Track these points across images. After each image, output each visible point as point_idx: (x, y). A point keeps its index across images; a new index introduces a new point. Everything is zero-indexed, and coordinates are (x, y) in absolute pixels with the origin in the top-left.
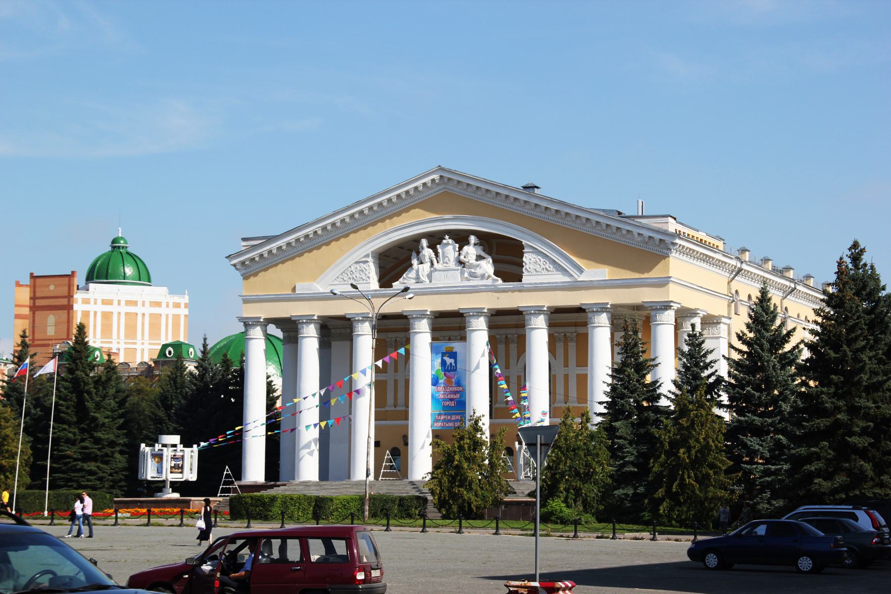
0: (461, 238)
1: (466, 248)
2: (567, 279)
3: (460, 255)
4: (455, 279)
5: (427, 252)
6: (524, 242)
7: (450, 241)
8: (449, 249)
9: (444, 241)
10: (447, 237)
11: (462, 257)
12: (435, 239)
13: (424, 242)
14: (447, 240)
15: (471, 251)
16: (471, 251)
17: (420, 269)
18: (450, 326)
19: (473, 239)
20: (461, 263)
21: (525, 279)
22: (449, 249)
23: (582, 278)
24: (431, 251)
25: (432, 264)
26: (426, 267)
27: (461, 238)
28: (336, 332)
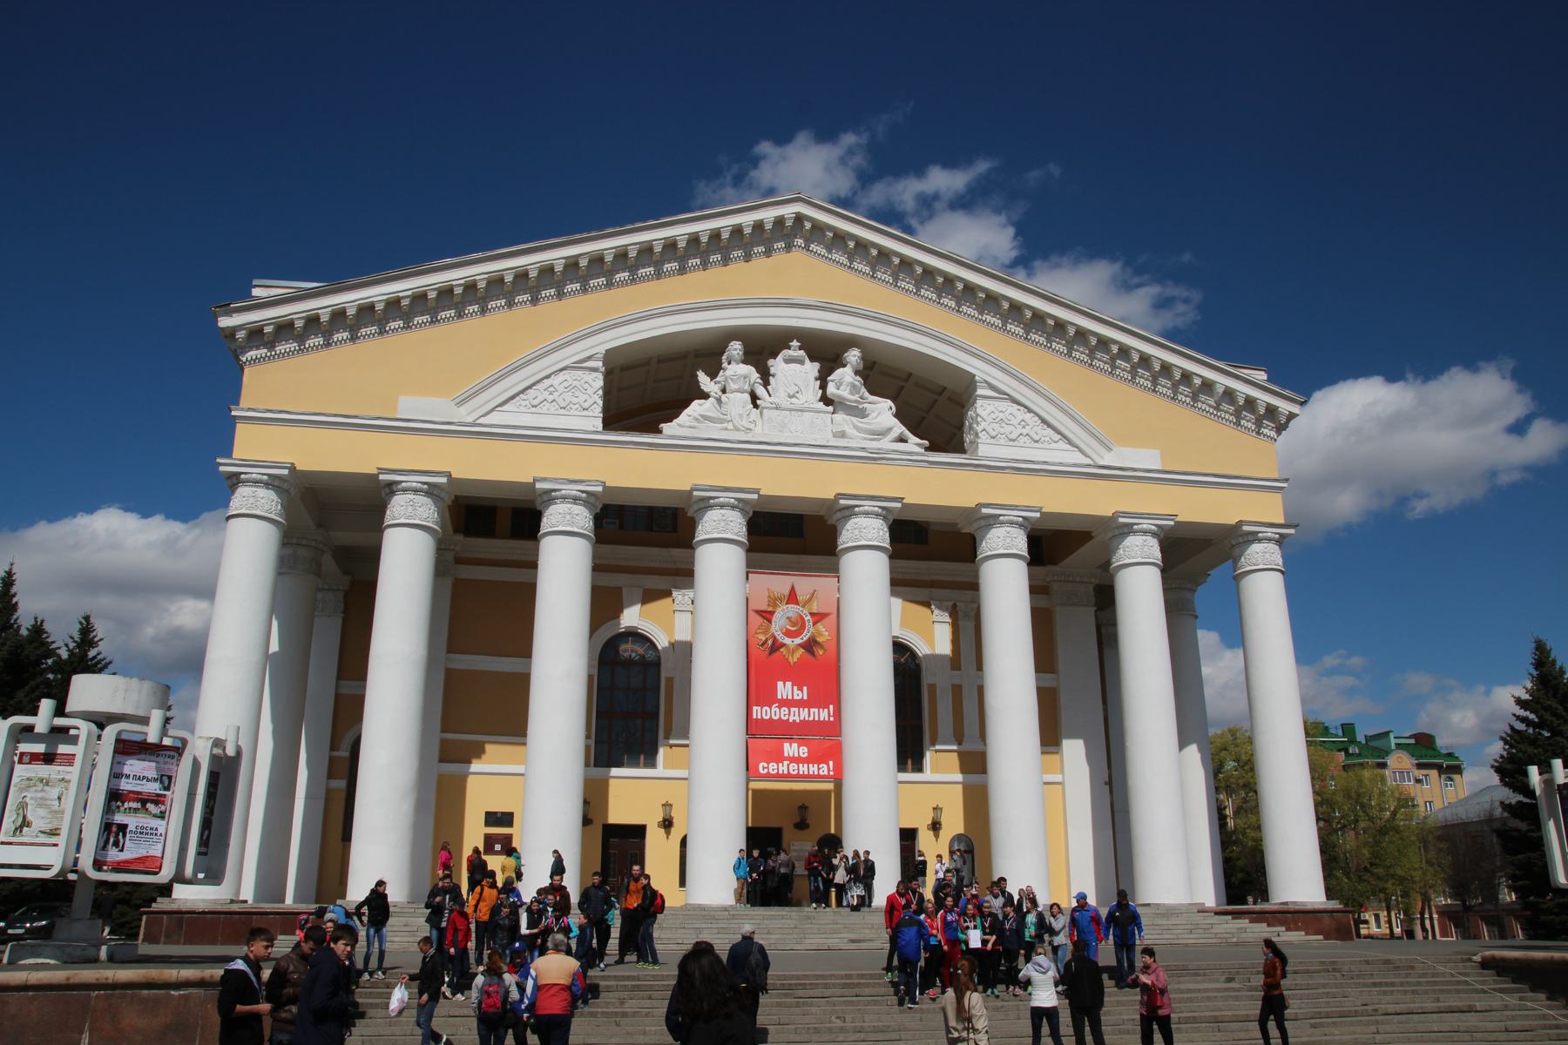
0: (826, 352)
1: (839, 371)
2: (1078, 458)
3: (823, 387)
4: (819, 427)
5: (737, 371)
6: (979, 376)
7: (802, 352)
8: (794, 374)
9: (785, 352)
10: (795, 343)
11: (831, 389)
12: (762, 349)
13: (736, 348)
14: (795, 350)
15: (845, 380)
16: (845, 380)
18: (791, 536)
19: (853, 356)
20: (826, 400)
21: (987, 449)
22: (794, 374)
23: (1108, 459)
24: (749, 370)
25: (754, 398)
26: (738, 401)
27: (826, 352)
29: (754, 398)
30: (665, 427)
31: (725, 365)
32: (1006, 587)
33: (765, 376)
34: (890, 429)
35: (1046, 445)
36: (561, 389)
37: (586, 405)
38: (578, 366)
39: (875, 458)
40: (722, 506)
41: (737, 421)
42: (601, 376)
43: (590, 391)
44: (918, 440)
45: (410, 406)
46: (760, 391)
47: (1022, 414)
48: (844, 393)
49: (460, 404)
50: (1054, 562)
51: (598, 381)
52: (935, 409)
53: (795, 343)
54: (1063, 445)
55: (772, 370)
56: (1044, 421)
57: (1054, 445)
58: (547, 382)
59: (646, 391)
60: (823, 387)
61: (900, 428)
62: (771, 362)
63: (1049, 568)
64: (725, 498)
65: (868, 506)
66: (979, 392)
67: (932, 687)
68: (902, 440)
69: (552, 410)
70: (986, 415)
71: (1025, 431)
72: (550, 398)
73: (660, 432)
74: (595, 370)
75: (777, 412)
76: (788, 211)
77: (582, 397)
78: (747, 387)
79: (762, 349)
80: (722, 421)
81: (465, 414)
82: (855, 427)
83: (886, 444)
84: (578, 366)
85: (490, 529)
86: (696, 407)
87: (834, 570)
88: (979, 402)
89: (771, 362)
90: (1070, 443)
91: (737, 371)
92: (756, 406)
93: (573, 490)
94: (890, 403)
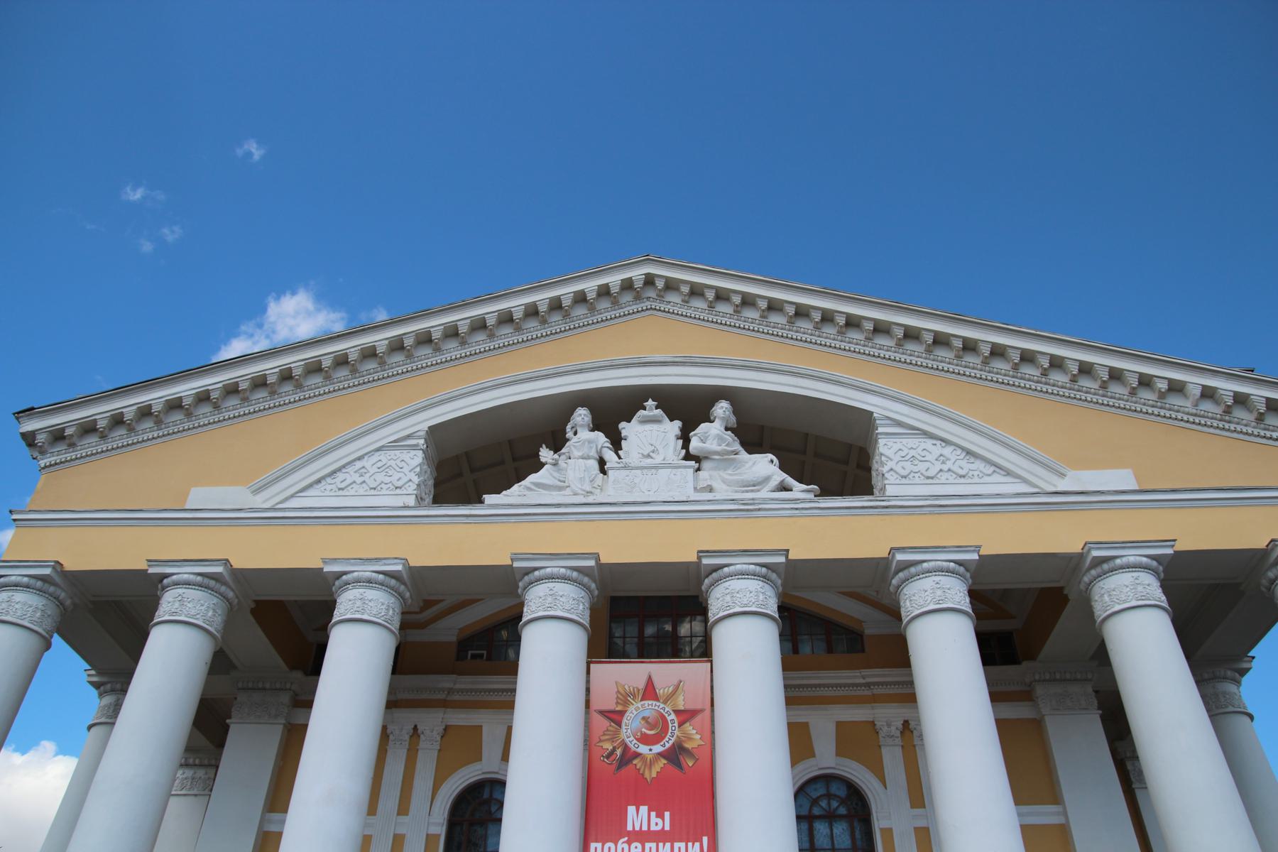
0: (687, 408)
1: (704, 427)
3: (686, 440)
4: (679, 483)
5: (584, 438)
6: (877, 413)
7: (659, 412)
9: (641, 412)
10: (650, 403)
11: (695, 444)
12: (611, 413)
13: (582, 416)
15: (713, 435)
16: (713, 435)
17: (569, 472)
18: (648, 616)
19: (722, 409)
24: (600, 438)
25: (602, 462)
27: (687, 408)
28: (279, 631)
29: (602, 462)
30: (489, 499)
31: (569, 434)
32: (945, 654)
33: (616, 442)
34: (767, 479)
35: (976, 480)
36: (374, 469)
37: (399, 484)
38: (396, 444)
39: (748, 510)
40: (551, 578)
41: (576, 486)
42: (420, 454)
43: (406, 469)
44: (804, 487)
45: (200, 497)
46: (610, 456)
47: (936, 449)
48: (712, 445)
49: (256, 492)
50: (1031, 656)
51: (417, 458)
52: (829, 454)
53: (650, 403)
54: (997, 478)
55: (624, 433)
56: (969, 453)
57: (987, 479)
58: (359, 464)
59: (474, 463)
60: (686, 440)
61: (780, 476)
62: (622, 425)
63: (1025, 664)
64: (553, 567)
65: (741, 563)
66: (880, 430)
67: (888, 833)
68: (783, 488)
69: (361, 492)
70: (892, 456)
71: (945, 467)
72: (360, 480)
73: (482, 502)
74: (414, 447)
75: (627, 472)
76: (637, 274)
77: (397, 476)
78: (593, 453)
79: (611, 413)
80: (560, 489)
81: (260, 501)
82: (724, 481)
83: (765, 493)
84: (396, 444)
85: (279, 631)
86: (532, 478)
87: (704, 651)
88: (881, 442)
89: (622, 425)
90: (1008, 473)
91: (584, 438)
92: (603, 471)
93: (366, 571)
94: (770, 456)
